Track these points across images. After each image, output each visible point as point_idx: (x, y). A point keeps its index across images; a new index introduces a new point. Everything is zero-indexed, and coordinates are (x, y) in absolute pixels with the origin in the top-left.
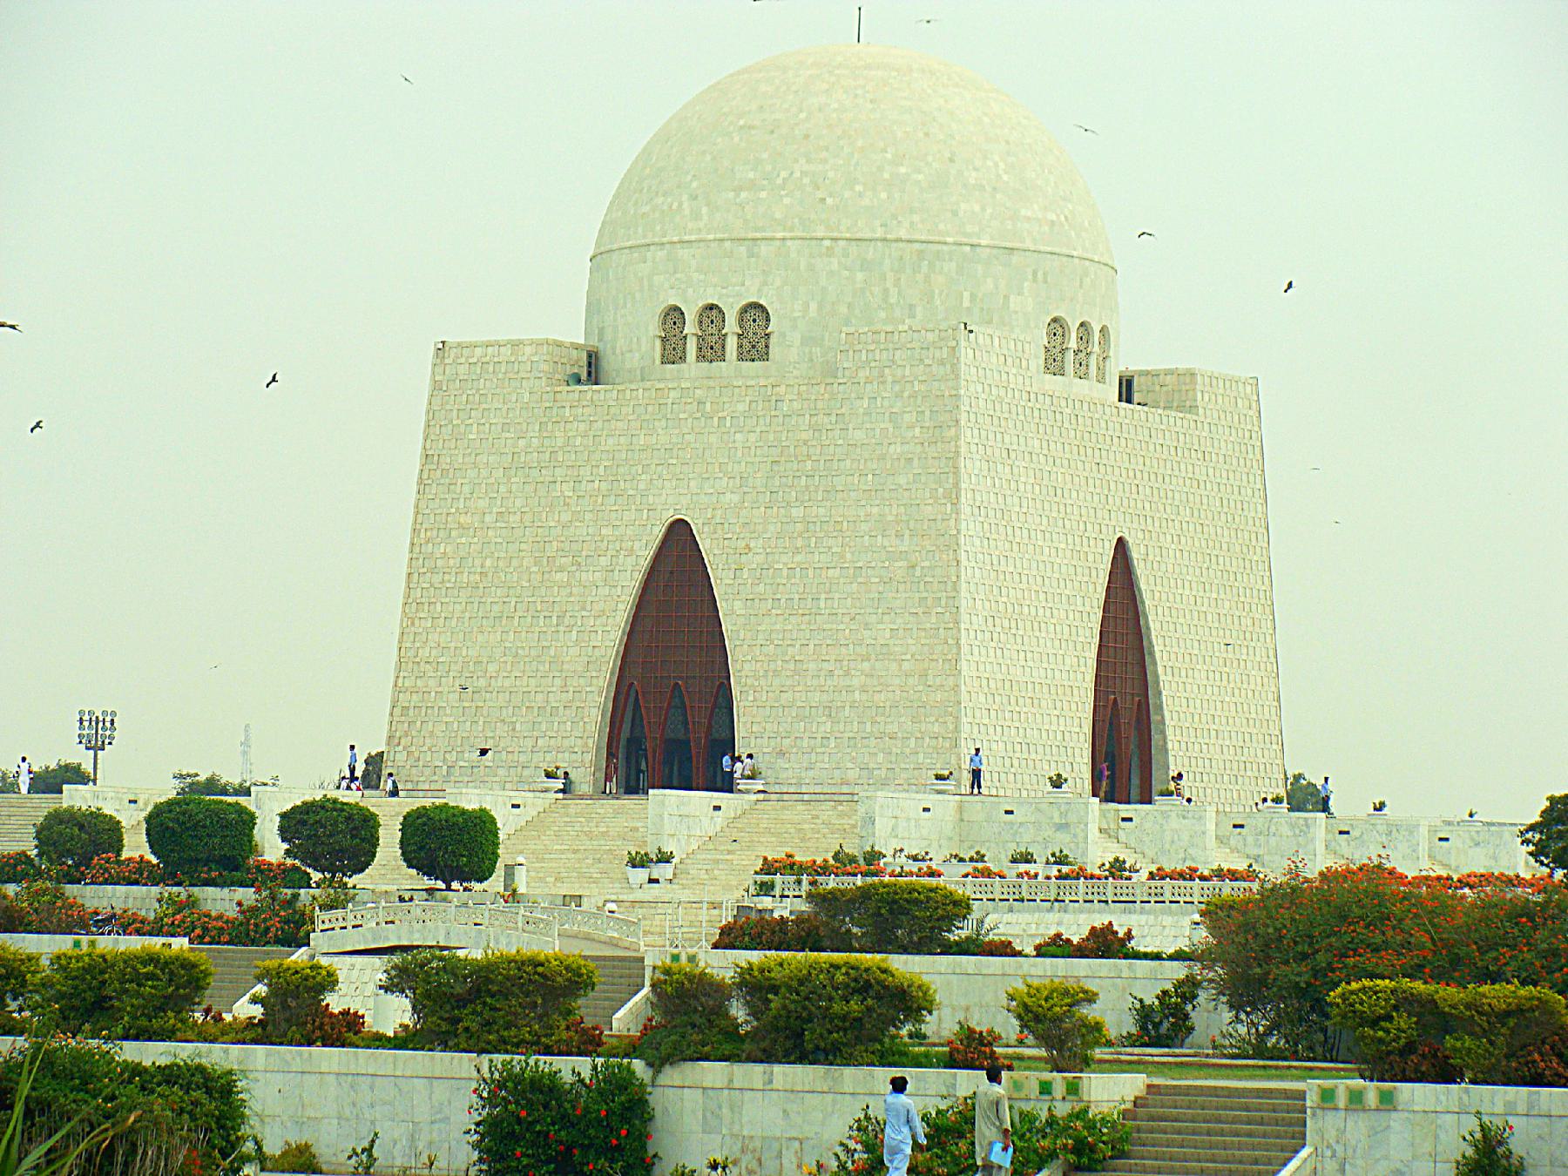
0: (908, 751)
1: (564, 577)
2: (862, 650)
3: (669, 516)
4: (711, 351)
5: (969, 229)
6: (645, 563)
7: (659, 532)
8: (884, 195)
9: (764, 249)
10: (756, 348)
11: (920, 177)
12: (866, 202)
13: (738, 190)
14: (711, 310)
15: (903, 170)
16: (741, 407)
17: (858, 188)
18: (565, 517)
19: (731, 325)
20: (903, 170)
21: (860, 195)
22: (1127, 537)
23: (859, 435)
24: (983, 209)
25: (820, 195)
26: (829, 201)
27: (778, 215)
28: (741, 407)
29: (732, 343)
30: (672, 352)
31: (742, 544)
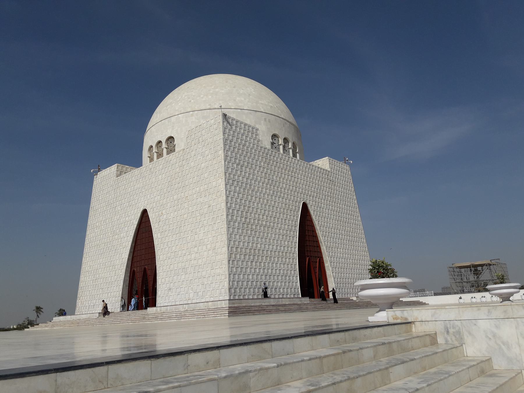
0: (209, 282)
1: (116, 236)
2: (194, 243)
3: (142, 210)
4: (160, 155)
5: (240, 104)
6: (135, 226)
7: (139, 215)
8: (210, 97)
9: (172, 118)
10: (171, 150)
11: (223, 91)
12: (204, 99)
13: (167, 106)
14: (160, 142)
15: (217, 90)
16: (161, 166)
17: (202, 96)
18: (118, 216)
19: (164, 145)
20: (217, 90)
21: (202, 98)
22: (308, 202)
23: (192, 164)
24: (245, 99)
25: (189, 100)
26: (192, 101)
27: (177, 109)
28: (161, 166)
29: (165, 151)
30: (151, 160)
31: (160, 212)
